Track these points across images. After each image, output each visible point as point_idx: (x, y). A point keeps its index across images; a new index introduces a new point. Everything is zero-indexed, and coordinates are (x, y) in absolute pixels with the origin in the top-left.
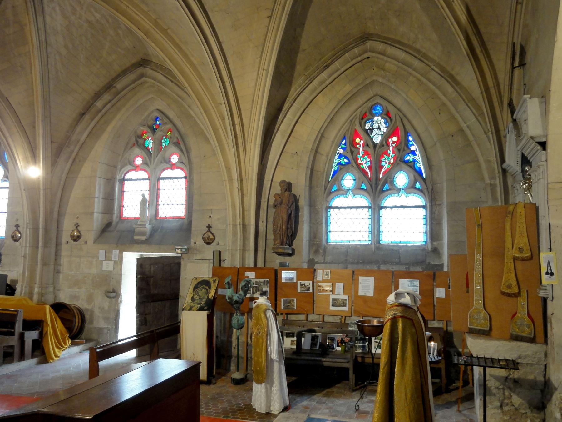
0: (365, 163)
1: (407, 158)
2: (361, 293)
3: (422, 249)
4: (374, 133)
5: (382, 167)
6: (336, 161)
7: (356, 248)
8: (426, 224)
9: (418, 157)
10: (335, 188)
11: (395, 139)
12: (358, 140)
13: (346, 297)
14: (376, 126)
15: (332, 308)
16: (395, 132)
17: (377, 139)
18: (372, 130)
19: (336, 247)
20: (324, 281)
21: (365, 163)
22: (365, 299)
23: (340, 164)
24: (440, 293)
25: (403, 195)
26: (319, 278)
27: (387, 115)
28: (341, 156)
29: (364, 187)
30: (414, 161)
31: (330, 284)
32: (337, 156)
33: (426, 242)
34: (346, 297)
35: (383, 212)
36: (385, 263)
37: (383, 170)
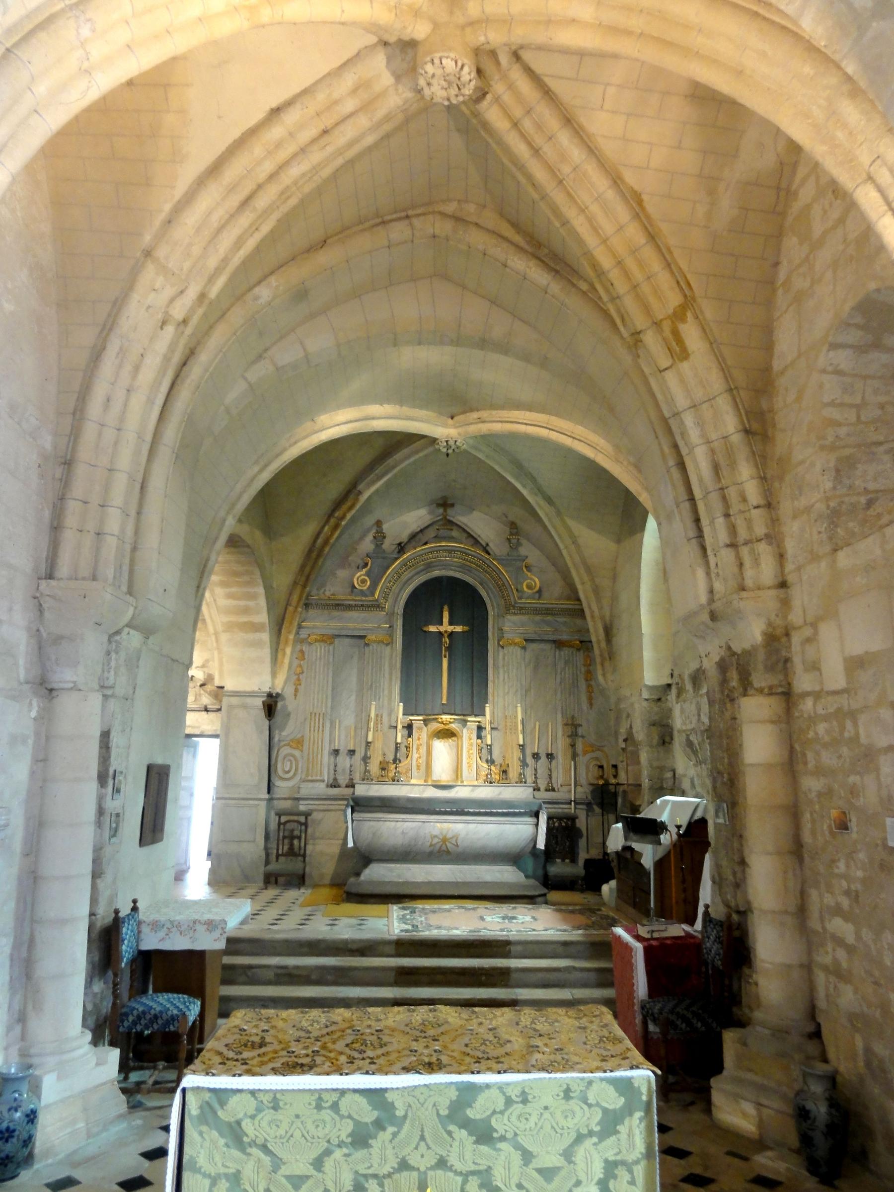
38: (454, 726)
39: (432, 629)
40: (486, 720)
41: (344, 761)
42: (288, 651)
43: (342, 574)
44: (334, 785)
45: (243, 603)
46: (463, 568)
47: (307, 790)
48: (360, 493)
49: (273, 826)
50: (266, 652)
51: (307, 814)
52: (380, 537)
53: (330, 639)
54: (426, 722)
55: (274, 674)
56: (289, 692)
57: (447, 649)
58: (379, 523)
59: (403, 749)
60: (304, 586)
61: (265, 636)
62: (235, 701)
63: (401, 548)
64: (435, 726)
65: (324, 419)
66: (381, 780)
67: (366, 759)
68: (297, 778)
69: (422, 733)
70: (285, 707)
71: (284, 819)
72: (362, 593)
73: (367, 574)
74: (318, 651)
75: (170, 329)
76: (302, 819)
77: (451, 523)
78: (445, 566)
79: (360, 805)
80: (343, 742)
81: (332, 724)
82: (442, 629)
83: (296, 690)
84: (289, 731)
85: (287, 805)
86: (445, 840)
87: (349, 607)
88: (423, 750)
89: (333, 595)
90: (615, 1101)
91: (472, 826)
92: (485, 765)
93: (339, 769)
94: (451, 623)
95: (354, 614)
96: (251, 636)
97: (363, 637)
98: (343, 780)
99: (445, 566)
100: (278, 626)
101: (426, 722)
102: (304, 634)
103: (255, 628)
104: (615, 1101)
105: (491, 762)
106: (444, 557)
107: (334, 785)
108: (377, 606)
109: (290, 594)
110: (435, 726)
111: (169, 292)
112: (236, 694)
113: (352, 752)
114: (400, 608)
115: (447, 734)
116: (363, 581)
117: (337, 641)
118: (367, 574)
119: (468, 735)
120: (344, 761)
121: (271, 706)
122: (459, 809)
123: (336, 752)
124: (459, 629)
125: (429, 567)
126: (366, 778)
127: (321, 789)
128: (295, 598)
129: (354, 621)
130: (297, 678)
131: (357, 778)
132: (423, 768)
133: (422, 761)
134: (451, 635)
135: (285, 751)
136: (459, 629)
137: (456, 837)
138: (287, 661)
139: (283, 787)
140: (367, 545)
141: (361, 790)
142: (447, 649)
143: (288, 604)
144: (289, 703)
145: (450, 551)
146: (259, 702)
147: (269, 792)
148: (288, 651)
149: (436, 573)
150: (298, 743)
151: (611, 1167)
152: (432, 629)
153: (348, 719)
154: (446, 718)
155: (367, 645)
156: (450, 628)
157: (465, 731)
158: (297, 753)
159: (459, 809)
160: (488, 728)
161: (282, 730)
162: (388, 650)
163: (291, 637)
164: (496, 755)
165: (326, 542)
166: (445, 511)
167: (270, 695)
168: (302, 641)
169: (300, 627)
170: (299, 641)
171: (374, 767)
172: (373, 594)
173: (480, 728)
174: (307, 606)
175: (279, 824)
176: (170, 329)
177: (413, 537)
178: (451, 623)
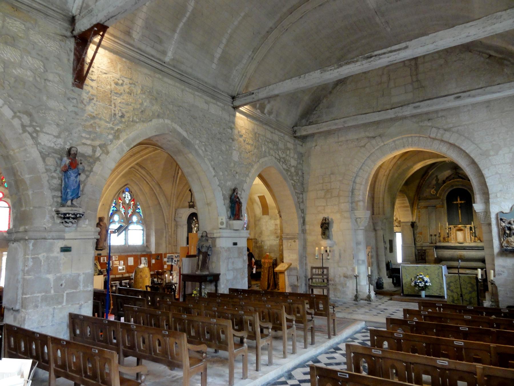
0: (122, 210)
1: (137, 211)
2: (129, 264)
3: (142, 246)
4: (126, 199)
5: (129, 213)
6: (112, 209)
7: (121, 246)
8: (143, 237)
9: (141, 211)
10: (111, 221)
11: (133, 202)
12: (120, 201)
13: (124, 266)
14: (126, 196)
15: (119, 271)
16: (133, 200)
17: (127, 202)
18: (125, 197)
19: (114, 246)
20: (116, 260)
21: (122, 210)
22: (131, 266)
23: (113, 210)
24: (153, 261)
25: (135, 225)
26: (114, 260)
27: (130, 192)
28: (114, 207)
29: (122, 221)
30: (139, 212)
31: (118, 261)
32: (112, 207)
33: (143, 243)
34: (124, 266)
35: (129, 231)
36: (134, 252)
37: (129, 215)
38: (462, 228)
39: (455, 202)
40: (472, 225)
41: (434, 238)
42: (416, 211)
43: (428, 190)
44: (432, 243)
45: (402, 202)
46: (462, 185)
47: (424, 244)
48: (429, 173)
49: (417, 253)
50: (410, 212)
51: (425, 250)
52: (437, 180)
53: (426, 207)
54: (454, 227)
55: (413, 217)
56: (417, 221)
57: (460, 207)
58: (437, 176)
59: (449, 234)
60: (418, 195)
61: (409, 209)
62: (403, 224)
63: (444, 182)
64: (457, 228)
65: (415, 167)
66: (443, 242)
67: (440, 237)
68: (421, 243)
69: (454, 230)
70: (417, 225)
71: (419, 251)
72: (433, 195)
73: (435, 190)
74: (423, 211)
75: (385, 176)
76: (424, 251)
77: (459, 173)
78: (456, 185)
79: (437, 248)
80: (433, 232)
81: (429, 229)
82: (458, 202)
83: (419, 221)
84: (418, 230)
85: (420, 248)
86: (461, 256)
87: (430, 199)
88: (454, 234)
89: (426, 196)
90: (439, 267)
91: (469, 253)
92: (473, 238)
93: (433, 240)
94: (460, 201)
95: (432, 201)
96: (406, 209)
97: (436, 206)
98: (434, 242)
99: (456, 185)
100: (412, 205)
101: (454, 227)
102: (419, 207)
103: (407, 207)
104: (439, 267)
105: (475, 236)
106: (457, 183)
107: (432, 243)
108: (438, 198)
109: (414, 198)
110: (457, 228)
111: (384, 171)
112: (403, 222)
113: (435, 235)
114: (445, 199)
115: (460, 230)
116: (434, 192)
117: (429, 208)
118: (435, 190)
119: (467, 230)
120: (434, 238)
121: (413, 225)
122: (464, 248)
123: (431, 235)
124: (463, 202)
125: (452, 186)
126: (440, 241)
127: (428, 244)
128: (416, 198)
129: (433, 202)
130: (419, 218)
131: (438, 241)
132: (455, 239)
133: (454, 237)
134: (461, 204)
135: (418, 235)
136: (463, 202)
137: (464, 255)
138: (416, 213)
139: (418, 244)
140: (434, 182)
141: (438, 244)
142: (460, 207)
143: (414, 200)
144: (418, 224)
145: (458, 181)
146: (410, 224)
147: (415, 245)
148: (416, 211)
149: (455, 187)
150: (421, 233)
151: (438, 273)
152: (455, 202)
153: (433, 227)
154: (460, 226)
155: (437, 208)
156: (460, 202)
157: (466, 229)
158: (421, 236)
159: (464, 248)
160: (473, 228)
161: (416, 230)
162: (443, 209)
163: (416, 208)
164: (477, 235)
165: (422, 184)
166: (456, 170)
167: (412, 222)
168: (419, 208)
169: (418, 205)
170: (418, 208)
171: (442, 239)
172: (437, 195)
173: (471, 228)
174: (419, 200)
175: (418, 252)
176: (385, 176)
177: (447, 178)
178: (460, 201)
